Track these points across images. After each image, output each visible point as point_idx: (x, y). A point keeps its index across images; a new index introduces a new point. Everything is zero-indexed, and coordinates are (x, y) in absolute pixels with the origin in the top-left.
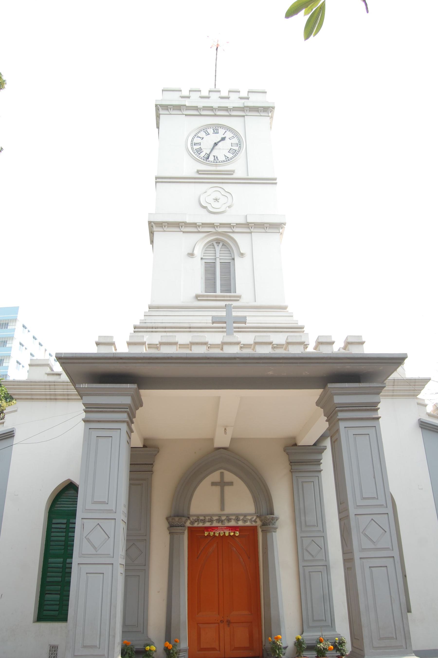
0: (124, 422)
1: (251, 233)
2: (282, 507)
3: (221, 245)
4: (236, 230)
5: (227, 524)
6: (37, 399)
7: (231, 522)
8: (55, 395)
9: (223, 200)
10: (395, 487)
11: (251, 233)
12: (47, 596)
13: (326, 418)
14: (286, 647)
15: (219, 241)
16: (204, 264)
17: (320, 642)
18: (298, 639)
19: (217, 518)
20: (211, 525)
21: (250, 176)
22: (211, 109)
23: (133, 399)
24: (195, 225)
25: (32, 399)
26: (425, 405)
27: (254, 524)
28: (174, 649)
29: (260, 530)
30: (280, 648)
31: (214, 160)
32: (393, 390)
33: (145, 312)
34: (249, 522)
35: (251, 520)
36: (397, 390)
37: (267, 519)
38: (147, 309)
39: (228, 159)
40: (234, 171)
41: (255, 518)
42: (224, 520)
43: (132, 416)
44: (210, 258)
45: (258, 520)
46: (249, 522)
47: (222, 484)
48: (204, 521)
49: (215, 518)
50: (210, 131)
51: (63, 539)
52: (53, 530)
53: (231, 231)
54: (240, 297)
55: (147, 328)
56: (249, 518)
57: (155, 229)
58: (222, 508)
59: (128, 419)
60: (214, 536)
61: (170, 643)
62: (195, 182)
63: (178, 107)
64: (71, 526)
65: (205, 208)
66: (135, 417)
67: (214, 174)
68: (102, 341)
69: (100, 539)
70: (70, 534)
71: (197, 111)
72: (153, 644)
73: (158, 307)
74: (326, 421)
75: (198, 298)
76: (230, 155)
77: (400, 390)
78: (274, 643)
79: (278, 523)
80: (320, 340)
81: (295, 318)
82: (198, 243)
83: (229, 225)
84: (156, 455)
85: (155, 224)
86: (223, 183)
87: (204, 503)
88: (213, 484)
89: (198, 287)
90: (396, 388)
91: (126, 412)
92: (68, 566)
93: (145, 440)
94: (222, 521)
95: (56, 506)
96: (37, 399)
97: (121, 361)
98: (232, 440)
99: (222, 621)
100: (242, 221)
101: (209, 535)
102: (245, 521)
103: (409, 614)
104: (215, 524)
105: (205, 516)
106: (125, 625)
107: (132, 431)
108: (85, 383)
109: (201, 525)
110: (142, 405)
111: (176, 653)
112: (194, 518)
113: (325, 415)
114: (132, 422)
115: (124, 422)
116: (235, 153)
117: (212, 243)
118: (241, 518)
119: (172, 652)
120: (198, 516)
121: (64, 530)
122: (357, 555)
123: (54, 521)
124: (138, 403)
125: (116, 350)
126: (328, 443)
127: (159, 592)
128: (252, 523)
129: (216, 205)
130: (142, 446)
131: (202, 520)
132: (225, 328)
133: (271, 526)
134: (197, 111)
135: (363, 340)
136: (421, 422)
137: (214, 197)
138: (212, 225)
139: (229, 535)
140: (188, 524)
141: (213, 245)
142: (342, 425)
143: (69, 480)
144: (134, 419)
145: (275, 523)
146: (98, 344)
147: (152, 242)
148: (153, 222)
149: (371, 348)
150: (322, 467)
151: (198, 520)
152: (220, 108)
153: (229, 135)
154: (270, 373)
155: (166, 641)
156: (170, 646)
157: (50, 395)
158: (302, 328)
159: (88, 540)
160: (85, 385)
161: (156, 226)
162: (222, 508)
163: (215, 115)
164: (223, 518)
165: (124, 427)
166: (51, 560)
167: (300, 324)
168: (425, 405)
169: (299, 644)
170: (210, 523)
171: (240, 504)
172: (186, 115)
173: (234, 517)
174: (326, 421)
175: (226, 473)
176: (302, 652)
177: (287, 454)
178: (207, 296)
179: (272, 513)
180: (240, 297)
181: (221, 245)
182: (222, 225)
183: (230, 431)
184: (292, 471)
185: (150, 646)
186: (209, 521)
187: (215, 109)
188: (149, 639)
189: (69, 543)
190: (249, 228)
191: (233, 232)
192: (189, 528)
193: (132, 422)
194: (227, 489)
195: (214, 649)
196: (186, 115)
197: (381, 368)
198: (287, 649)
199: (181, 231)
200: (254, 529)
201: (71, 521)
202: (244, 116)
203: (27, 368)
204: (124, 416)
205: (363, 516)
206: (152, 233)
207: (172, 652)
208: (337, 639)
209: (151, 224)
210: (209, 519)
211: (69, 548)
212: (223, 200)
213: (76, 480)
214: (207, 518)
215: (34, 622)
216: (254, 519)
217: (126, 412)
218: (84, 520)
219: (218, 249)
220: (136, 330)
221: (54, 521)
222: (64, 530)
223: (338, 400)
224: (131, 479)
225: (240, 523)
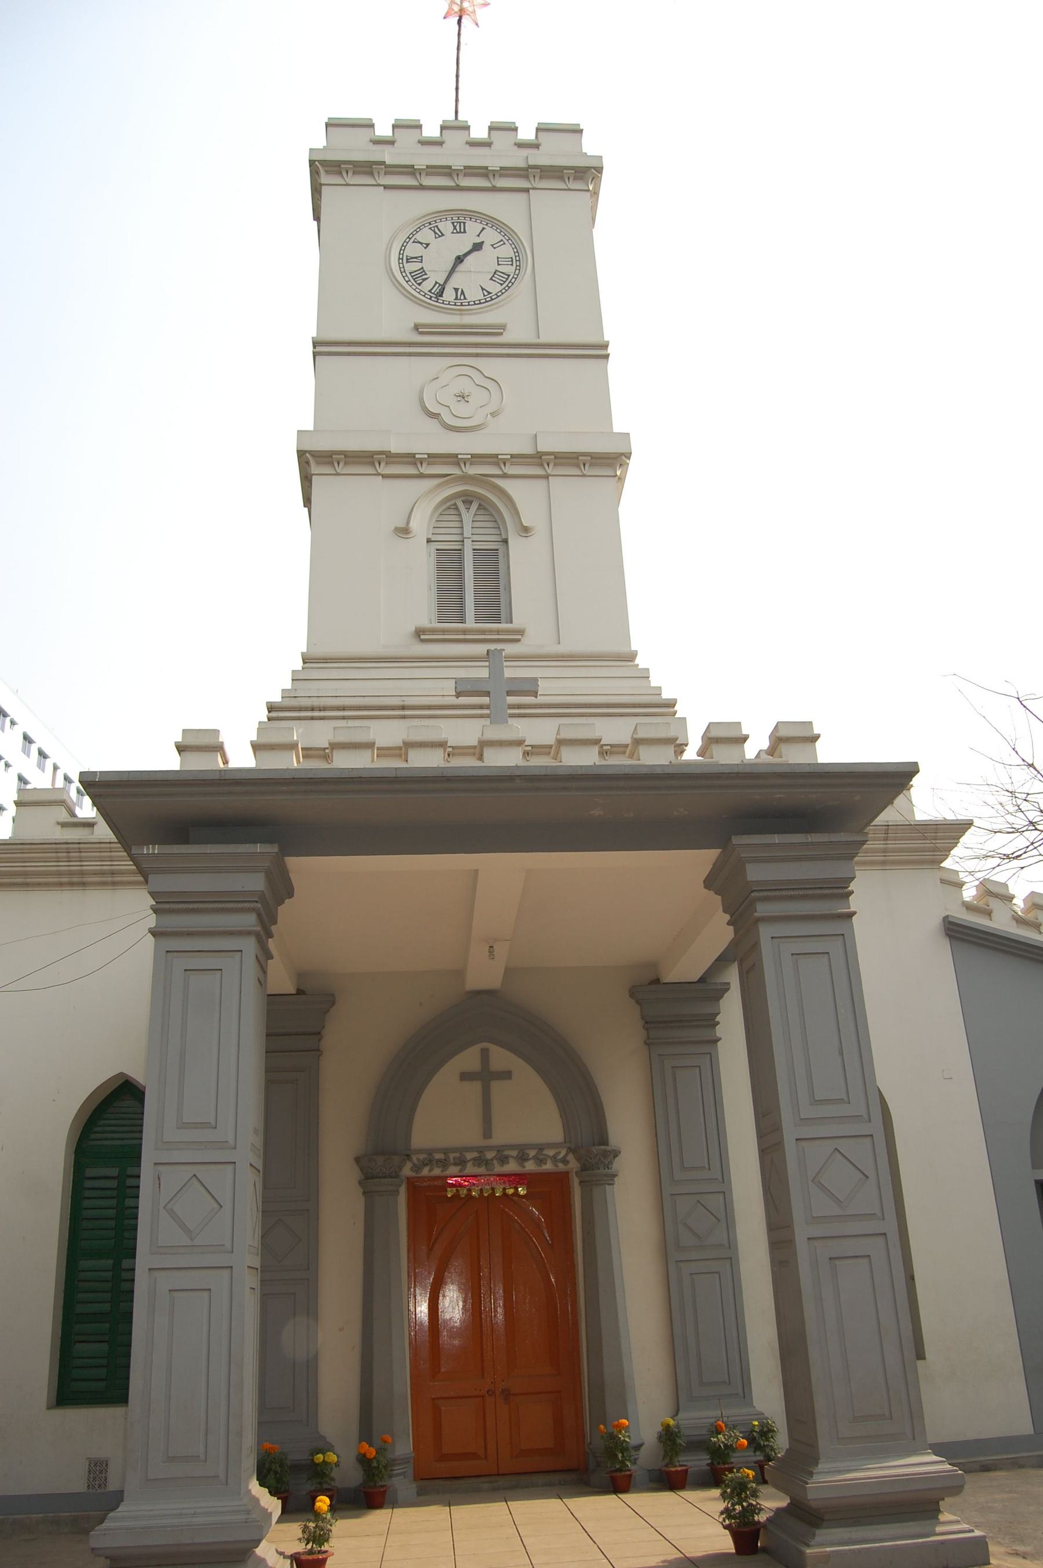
0: (249, 933)
1: (547, 477)
2: (628, 1128)
3: (474, 507)
4: (510, 470)
5: (498, 1169)
6: (39, 884)
7: (508, 1163)
8: (82, 873)
9: (478, 397)
10: (887, 1077)
11: (547, 477)
12: (78, 1345)
13: (727, 917)
14: (641, 1445)
15: (470, 498)
16: (434, 553)
17: (718, 1431)
18: (667, 1428)
19: (475, 1155)
20: (460, 1171)
21: (543, 339)
22: (447, 171)
23: (270, 879)
24: (410, 459)
25: (27, 884)
26: (960, 885)
27: (561, 1167)
28: (381, 1459)
29: (575, 1182)
30: (627, 1449)
31: (456, 298)
32: (885, 851)
33: (293, 672)
34: (549, 1162)
35: (554, 1158)
36: (894, 851)
37: (594, 1155)
38: (299, 665)
39: (489, 297)
40: (503, 327)
41: (563, 1152)
42: (492, 1159)
43: (267, 920)
44: (448, 538)
45: (571, 1157)
46: (549, 1162)
47: (486, 1076)
48: (444, 1164)
49: (469, 1156)
50: (446, 227)
51: (111, 1213)
52: (87, 1194)
53: (498, 472)
54: (521, 632)
55: (300, 709)
56: (551, 1153)
57: (314, 469)
58: (487, 1133)
59: (259, 928)
60: (469, 1195)
61: (371, 1445)
62: (410, 354)
63: (366, 168)
64: (130, 1182)
65: (435, 416)
66: (275, 923)
67: (455, 334)
68: (192, 741)
69: (197, 1213)
70: (129, 1202)
71: (411, 177)
72: (331, 1448)
73: (326, 660)
74: (729, 923)
75: (422, 637)
76: (494, 288)
77: (901, 850)
78: (612, 1437)
79: (616, 1165)
80: (714, 733)
81: (654, 682)
82: (419, 502)
83: (493, 459)
84: (328, 1011)
85: (313, 456)
86: (477, 355)
87: (444, 1119)
88: (465, 1076)
89: (423, 610)
90: (891, 845)
91: (253, 910)
92: (125, 1275)
93: (301, 976)
94: (487, 1163)
95: (93, 1136)
96: (39, 884)
97: (238, 789)
98: (509, 971)
99: (491, 1392)
100: (527, 449)
101: (456, 1196)
102: (540, 1161)
103: (920, 1363)
104: (470, 1169)
105: (446, 1151)
106: (263, 1407)
107: (269, 956)
108: (154, 844)
109: (437, 1172)
110: (290, 894)
111: (385, 1467)
112: (422, 1157)
113: (725, 911)
114: (270, 935)
115: (249, 933)
116: (507, 282)
117: (453, 502)
118: (532, 1153)
119: (375, 1464)
120: (430, 1152)
121: (114, 1193)
122: (801, 1233)
123: (90, 1172)
124: (281, 888)
125: (226, 762)
126: (732, 976)
127: (341, 1330)
128: (557, 1166)
129: (461, 409)
130: (294, 992)
131: (438, 1161)
132: (488, 707)
133: (602, 1171)
134: (411, 177)
135: (816, 732)
136: (950, 923)
137: (457, 392)
138: (453, 459)
139: (505, 1194)
140: (407, 1171)
141: (457, 509)
142: (765, 932)
143: (122, 1074)
144: (273, 927)
145: (611, 1163)
146: (181, 748)
147: (307, 501)
148: (309, 452)
149: (832, 751)
150: (719, 1031)
151: (429, 1162)
152: (470, 171)
153: (490, 236)
154: (597, 812)
155: (360, 1441)
156: (372, 1453)
157: (71, 873)
158: (671, 704)
159: (172, 1214)
160: (154, 849)
161: (318, 463)
162: (487, 1133)
163: (458, 188)
164: (490, 1155)
165: (249, 946)
166: (84, 1264)
167: (666, 695)
168: (960, 885)
169: (669, 1437)
170: (459, 1168)
171: (530, 1120)
172: (386, 187)
173: (514, 1153)
174: (729, 923)
175: (495, 1051)
176: (677, 1454)
177: (638, 1002)
178: (444, 631)
179: (604, 1141)
180: (521, 632)
181: (474, 507)
182: (477, 459)
183: (502, 950)
184: (648, 1043)
185: (324, 1453)
186: (455, 1164)
187: (458, 172)
188: (322, 1438)
189: (126, 1222)
190: (542, 465)
191: (505, 476)
192: (410, 1181)
193: (270, 935)
194: (497, 1087)
195: (474, 1456)
196: (386, 187)
197: (858, 798)
198: (643, 1448)
199: (379, 474)
200: (561, 1180)
201: (130, 1171)
202: (527, 190)
203: (11, 810)
204: (250, 921)
205: (818, 1142)
206: (306, 480)
207: (375, 1464)
208: (756, 1423)
209: (305, 458)
210: (455, 1158)
211: (126, 1234)
212: (478, 397)
213: (138, 1075)
214: (452, 1156)
215: (49, 1408)
216: (561, 1156)
217: (253, 910)
218: (161, 1168)
219: (467, 517)
220: (274, 714)
221: (90, 1172)
222: (114, 1193)
223: (755, 873)
224: (268, 1070)
225: (530, 1166)
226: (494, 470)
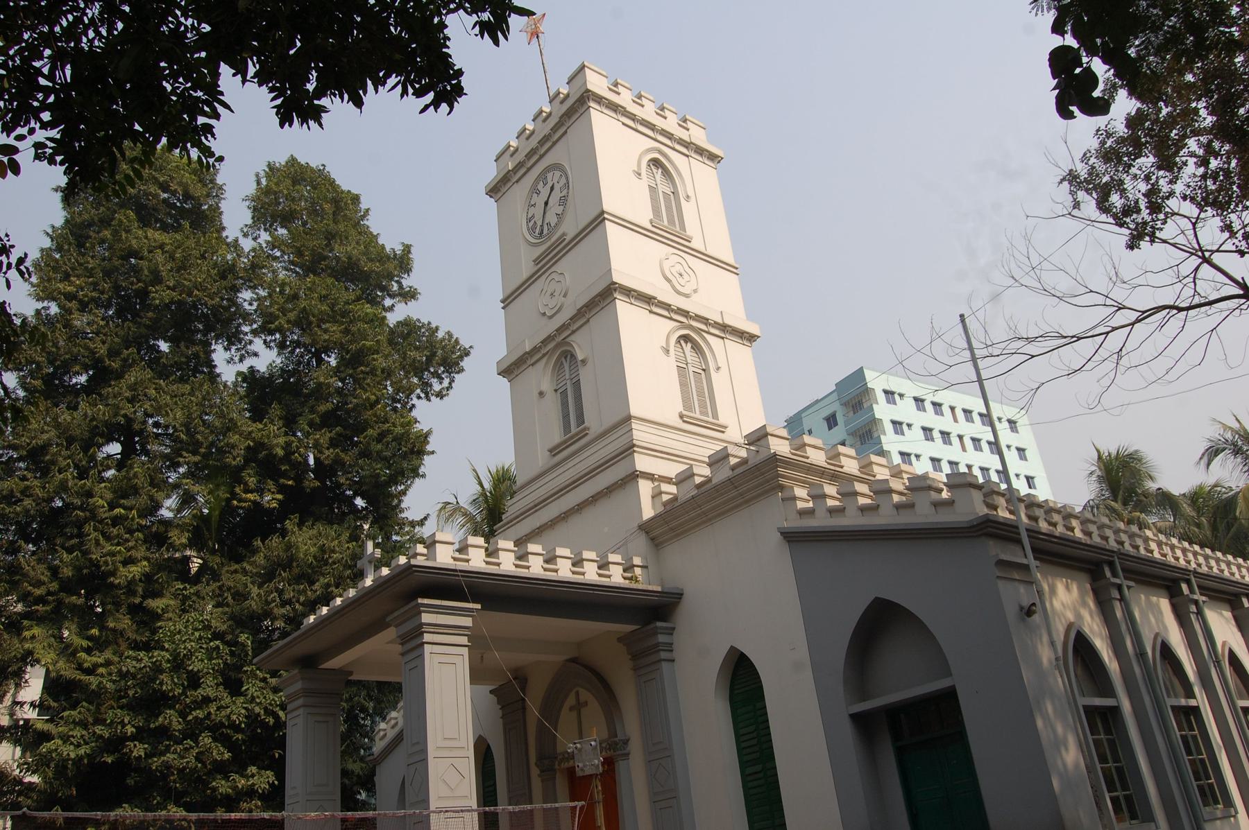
24: (667, 307)
63: (615, 108)
65: (669, 280)
83: (705, 321)
129: (680, 280)
138: (685, 313)
182: (699, 318)
226: (703, 327)
